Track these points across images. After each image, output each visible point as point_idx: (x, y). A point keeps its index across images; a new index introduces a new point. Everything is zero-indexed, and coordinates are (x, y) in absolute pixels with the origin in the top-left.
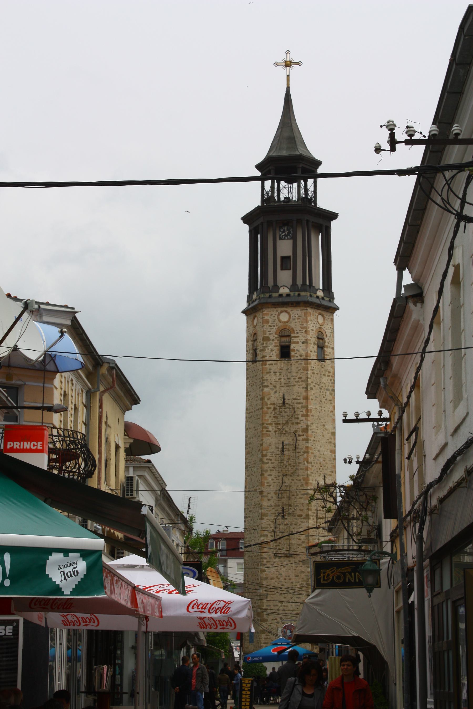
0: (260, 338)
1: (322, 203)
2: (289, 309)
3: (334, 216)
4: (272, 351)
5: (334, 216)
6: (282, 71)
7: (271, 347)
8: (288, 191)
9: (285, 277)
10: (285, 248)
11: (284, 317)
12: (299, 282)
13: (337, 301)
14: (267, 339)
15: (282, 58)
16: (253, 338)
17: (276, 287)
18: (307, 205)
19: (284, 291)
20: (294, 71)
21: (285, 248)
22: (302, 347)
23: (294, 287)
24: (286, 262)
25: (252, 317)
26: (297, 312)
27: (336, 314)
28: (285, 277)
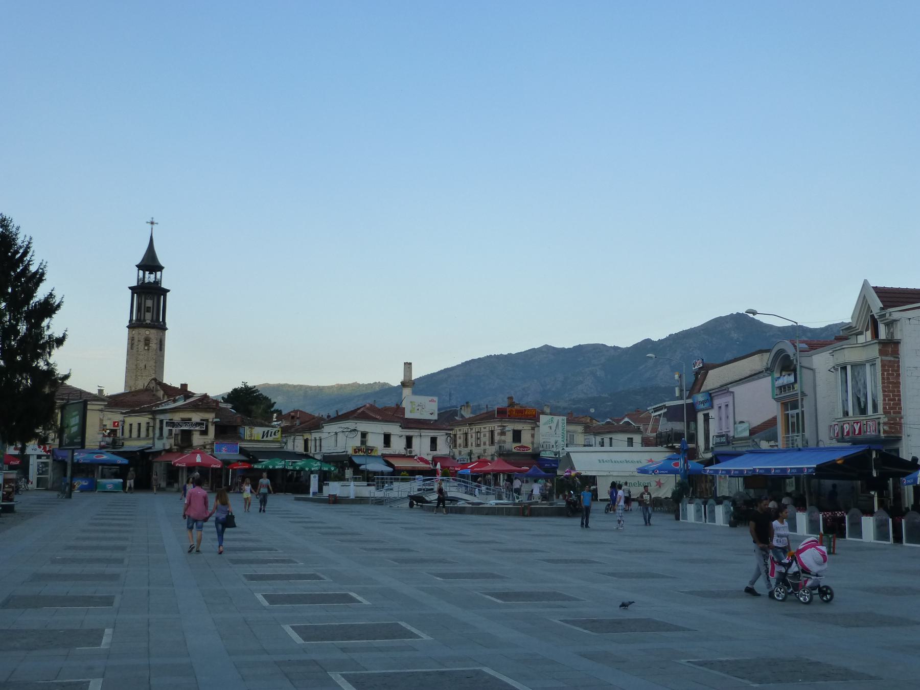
0: (136, 339)
1: (164, 285)
3: (168, 291)
4: (141, 346)
5: (168, 291)
6: (149, 226)
8: (150, 278)
10: (149, 303)
11: (147, 332)
12: (155, 318)
13: (167, 326)
16: (131, 341)
17: (145, 320)
18: (157, 283)
19: (148, 322)
20: (155, 226)
21: (149, 303)
22: (154, 345)
23: (152, 320)
26: (153, 331)
28: (148, 316)
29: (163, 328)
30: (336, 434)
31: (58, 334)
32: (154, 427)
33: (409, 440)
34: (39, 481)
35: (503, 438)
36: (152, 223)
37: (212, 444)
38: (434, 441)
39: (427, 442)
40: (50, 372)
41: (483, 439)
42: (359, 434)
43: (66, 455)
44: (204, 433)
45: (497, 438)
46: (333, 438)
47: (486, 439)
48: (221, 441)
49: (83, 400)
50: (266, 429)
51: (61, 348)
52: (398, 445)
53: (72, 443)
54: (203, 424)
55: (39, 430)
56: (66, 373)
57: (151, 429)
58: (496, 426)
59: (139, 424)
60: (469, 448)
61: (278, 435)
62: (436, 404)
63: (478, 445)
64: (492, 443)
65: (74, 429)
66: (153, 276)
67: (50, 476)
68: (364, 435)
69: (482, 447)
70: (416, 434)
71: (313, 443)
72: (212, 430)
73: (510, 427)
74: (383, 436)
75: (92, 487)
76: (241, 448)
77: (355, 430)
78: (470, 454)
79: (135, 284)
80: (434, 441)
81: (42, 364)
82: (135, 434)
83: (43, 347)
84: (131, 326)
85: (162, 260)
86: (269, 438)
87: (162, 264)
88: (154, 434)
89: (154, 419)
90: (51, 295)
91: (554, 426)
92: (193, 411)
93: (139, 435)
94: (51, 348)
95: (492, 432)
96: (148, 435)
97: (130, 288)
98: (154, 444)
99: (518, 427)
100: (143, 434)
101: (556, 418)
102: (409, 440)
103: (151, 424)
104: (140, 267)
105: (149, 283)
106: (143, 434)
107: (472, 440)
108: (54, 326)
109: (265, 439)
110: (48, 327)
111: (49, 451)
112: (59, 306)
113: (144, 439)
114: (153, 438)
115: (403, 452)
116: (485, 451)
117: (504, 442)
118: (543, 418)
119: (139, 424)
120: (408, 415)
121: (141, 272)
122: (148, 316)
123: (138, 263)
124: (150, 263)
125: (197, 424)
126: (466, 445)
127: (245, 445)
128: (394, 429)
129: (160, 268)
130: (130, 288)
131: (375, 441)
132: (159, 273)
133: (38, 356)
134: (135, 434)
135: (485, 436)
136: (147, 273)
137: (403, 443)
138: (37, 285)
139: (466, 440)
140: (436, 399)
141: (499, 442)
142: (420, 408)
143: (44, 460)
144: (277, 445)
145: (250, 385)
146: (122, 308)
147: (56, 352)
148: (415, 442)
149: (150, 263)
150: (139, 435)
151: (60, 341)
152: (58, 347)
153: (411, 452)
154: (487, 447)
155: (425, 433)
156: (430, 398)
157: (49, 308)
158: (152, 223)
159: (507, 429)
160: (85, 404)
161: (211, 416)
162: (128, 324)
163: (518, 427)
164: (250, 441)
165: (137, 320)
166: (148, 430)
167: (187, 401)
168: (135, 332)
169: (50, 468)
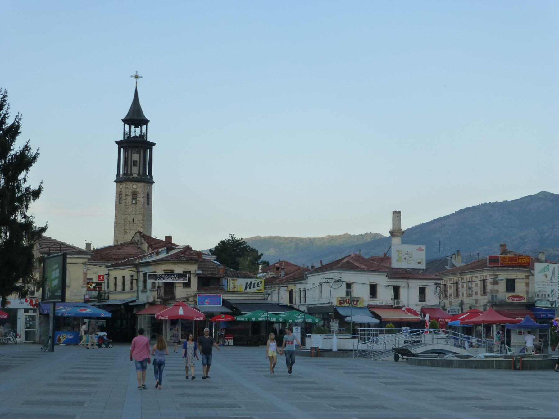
0: (124, 194)
1: (150, 139)
2: (137, 183)
3: (154, 144)
5: (154, 144)
6: (134, 80)
7: (129, 198)
8: (136, 132)
9: (135, 170)
10: (136, 157)
11: (135, 186)
12: (141, 172)
13: (154, 180)
14: (127, 195)
15: (134, 74)
17: (131, 174)
18: (143, 137)
20: (139, 80)
21: (136, 157)
22: (141, 199)
23: (139, 174)
24: (135, 163)
25: (119, 184)
26: (140, 185)
27: (153, 185)
28: (135, 170)
29: (149, 181)
30: (321, 284)
31: (34, 187)
32: (138, 280)
33: (396, 291)
34: (28, 335)
35: (496, 287)
36: (137, 77)
37: (195, 296)
38: (422, 291)
39: (415, 293)
40: (28, 225)
41: (475, 289)
42: (344, 285)
43: (48, 308)
44: (187, 285)
45: (489, 287)
46: (317, 291)
47: (478, 289)
48: (203, 293)
49: (64, 252)
50: (249, 281)
51: (37, 200)
52: (385, 296)
53: (53, 297)
54: (185, 276)
55: (19, 283)
56: (43, 225)
57: (135, 282)
58: (488, 275)
59: (124, 277)
60: (460, 299)
61: (262, 287)
62: (424, 252)
63: (470, 295)
64: (485, 292)
65: (56, 283)
66: (138, 130)
67: (37, 329)
68: (349, 286)
69: (474, 297)
70: (404, 284)
71: (298, 294)
72: (194, 282)
73: (503, 276)
74: (369, 286)
75: (76, 341)
76: (224, 300)
77: (339, 281)
78: (461, 304)
79: (121, 138)
80: (422, 291)
81: (19, 218)
82: (119, 288)
83: (20, 200)
84: (118, 181)
85: (147, 114)
86: (252, 290)
87: (148, 119)
88: (138, 287)
89: (138, 272)
90: (27, 148)
91: (549, 274)
92: (176, 263)
93: (124, 289)
94: (28, 200)
95: (484, 281)
96: (132, 288)
97: (117, 142)
98: (138, 297)
99: (512, 275)
100: (127, 287)
101: (551, 266)
102: (396, 291)
103: (135, 277)
104: (125, 121)
105: (135, 137)
106: (127, 287)
107: (463, 290)
108: (30, 179)
109: (248, 290)
110: (25, 180)
111: (36, 305)
112: (34, 158)
113: (128, 292)
114: (138, 291)
115: (390, 303)
116: (477, 301)
117: (497, 291)
118: (538, 266)
119: (124, 277)
120: (394, 264)
121: (127, 126)
122: (135, 170)
123: (123, 117)
124: (136, 117)
125: (180, 276)
126: (457, 295)
127: (227, 297)
128: (380, 279)
129: (146, 122)
130: (117, 142)
131: (361, 292)
132: (144, 127)
133: (14, 210)
134: (119, 288)
135: (476, 285)
136: (133, 127)
137: (390, 293)
138: (13, 138)
139: (457, 290)
140: (424, 247)
141: (492, 291)
142: (407, 257)
143: (31, 313)
144: (260, 297)
145: (237, 237)
146: (109, 162)
147: (32, 204)
148: (403, 292)
149: (136, 117)
150: (124, 289)
151: (36, 194)
152: (34, 200)
153: (398, 303)
154: (479, 297)
155: (412, 283)
156: (418, 246)
157: (25, 161)
158: (137, 77)
159: (500, 278)
160: (64, 256)
161: (193, 268)
162: (115, 178)
163: (512, 275)
164: (234, 292)
165: (125, 174)
166: (132, 283)
167: (171, 253)
168: (123, 186)
169: (37, 322)
